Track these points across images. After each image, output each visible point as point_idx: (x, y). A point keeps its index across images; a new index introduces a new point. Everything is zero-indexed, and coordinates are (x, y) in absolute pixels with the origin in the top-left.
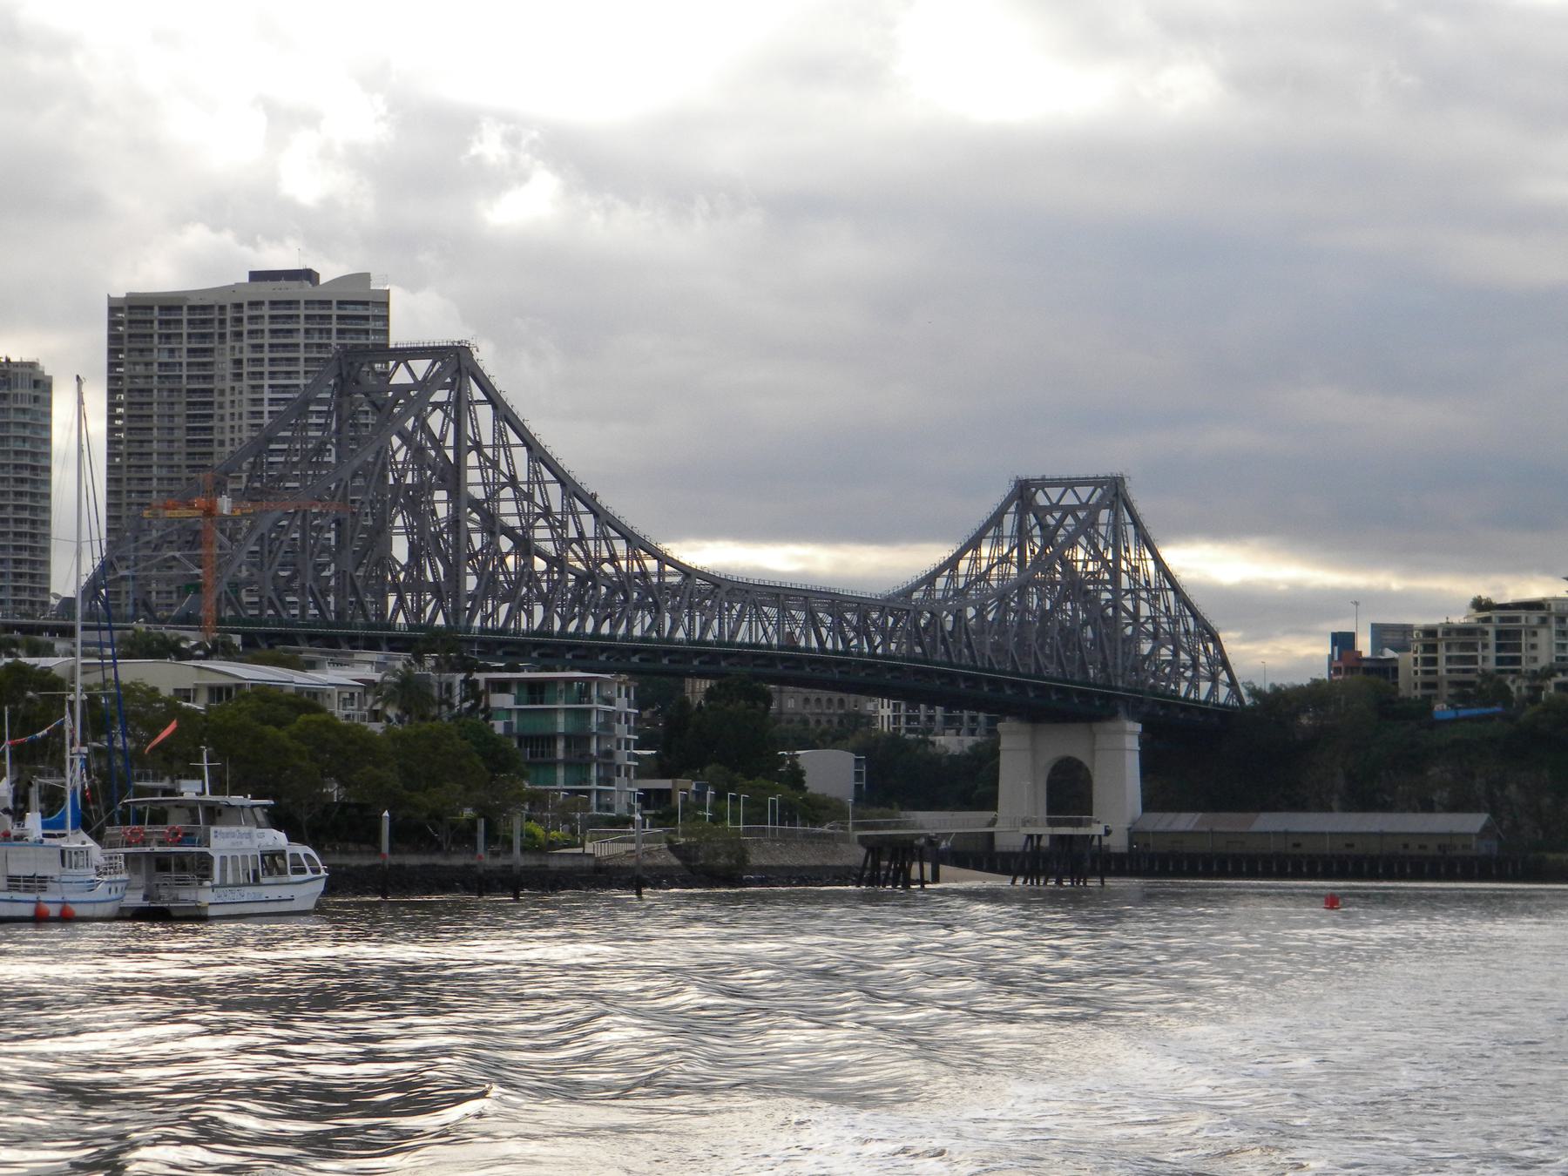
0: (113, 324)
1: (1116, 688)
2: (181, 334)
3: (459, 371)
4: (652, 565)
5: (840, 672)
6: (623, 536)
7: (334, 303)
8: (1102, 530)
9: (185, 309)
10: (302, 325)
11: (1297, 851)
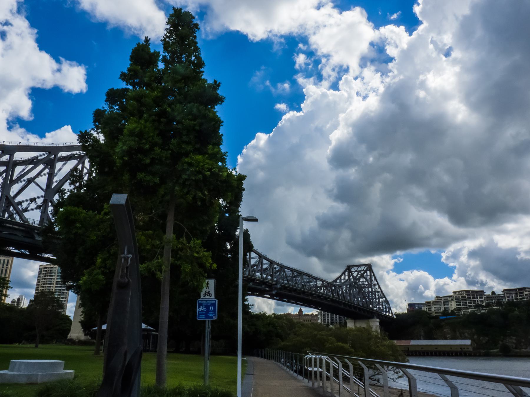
11: (422, 350)
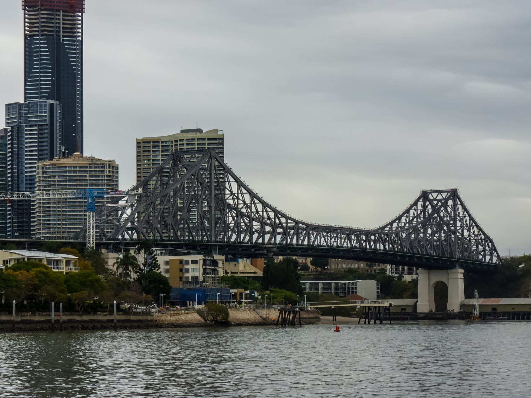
0: (138, 147)
1: (455, 258)
2: (159, 150)
3: (211, 157)
4: (283, 220)
5: (353, 254)
6: (273, 211)
7: (206, 139)
8: (450, 206)
9: (160, 142)
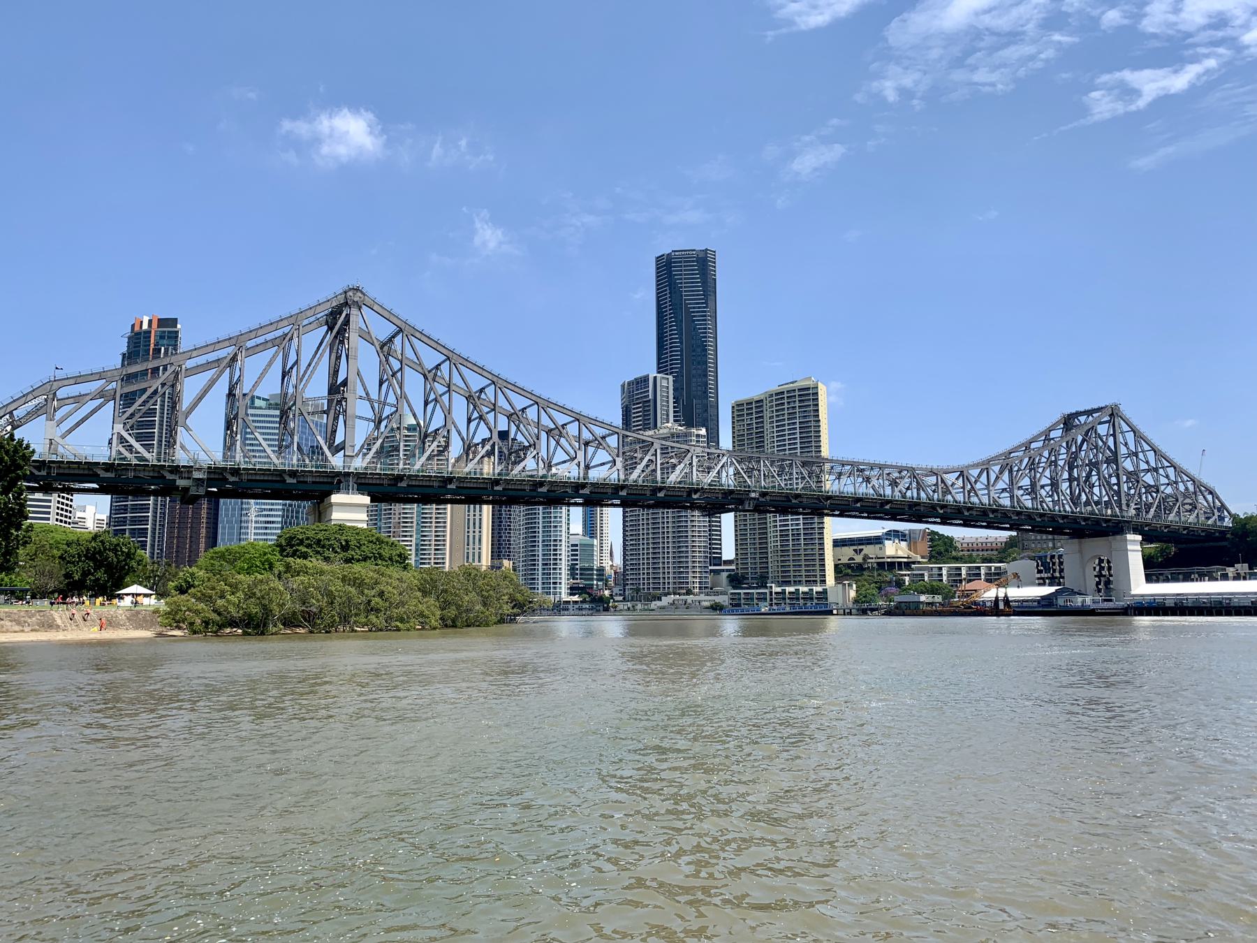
10: (786, 401)
